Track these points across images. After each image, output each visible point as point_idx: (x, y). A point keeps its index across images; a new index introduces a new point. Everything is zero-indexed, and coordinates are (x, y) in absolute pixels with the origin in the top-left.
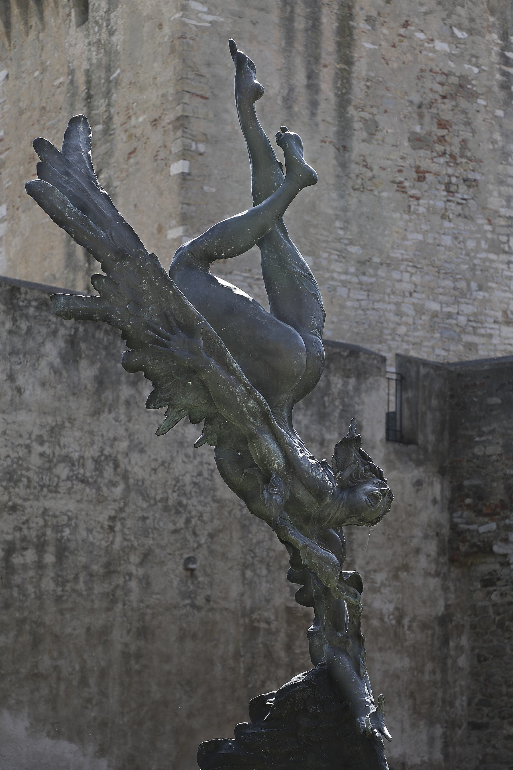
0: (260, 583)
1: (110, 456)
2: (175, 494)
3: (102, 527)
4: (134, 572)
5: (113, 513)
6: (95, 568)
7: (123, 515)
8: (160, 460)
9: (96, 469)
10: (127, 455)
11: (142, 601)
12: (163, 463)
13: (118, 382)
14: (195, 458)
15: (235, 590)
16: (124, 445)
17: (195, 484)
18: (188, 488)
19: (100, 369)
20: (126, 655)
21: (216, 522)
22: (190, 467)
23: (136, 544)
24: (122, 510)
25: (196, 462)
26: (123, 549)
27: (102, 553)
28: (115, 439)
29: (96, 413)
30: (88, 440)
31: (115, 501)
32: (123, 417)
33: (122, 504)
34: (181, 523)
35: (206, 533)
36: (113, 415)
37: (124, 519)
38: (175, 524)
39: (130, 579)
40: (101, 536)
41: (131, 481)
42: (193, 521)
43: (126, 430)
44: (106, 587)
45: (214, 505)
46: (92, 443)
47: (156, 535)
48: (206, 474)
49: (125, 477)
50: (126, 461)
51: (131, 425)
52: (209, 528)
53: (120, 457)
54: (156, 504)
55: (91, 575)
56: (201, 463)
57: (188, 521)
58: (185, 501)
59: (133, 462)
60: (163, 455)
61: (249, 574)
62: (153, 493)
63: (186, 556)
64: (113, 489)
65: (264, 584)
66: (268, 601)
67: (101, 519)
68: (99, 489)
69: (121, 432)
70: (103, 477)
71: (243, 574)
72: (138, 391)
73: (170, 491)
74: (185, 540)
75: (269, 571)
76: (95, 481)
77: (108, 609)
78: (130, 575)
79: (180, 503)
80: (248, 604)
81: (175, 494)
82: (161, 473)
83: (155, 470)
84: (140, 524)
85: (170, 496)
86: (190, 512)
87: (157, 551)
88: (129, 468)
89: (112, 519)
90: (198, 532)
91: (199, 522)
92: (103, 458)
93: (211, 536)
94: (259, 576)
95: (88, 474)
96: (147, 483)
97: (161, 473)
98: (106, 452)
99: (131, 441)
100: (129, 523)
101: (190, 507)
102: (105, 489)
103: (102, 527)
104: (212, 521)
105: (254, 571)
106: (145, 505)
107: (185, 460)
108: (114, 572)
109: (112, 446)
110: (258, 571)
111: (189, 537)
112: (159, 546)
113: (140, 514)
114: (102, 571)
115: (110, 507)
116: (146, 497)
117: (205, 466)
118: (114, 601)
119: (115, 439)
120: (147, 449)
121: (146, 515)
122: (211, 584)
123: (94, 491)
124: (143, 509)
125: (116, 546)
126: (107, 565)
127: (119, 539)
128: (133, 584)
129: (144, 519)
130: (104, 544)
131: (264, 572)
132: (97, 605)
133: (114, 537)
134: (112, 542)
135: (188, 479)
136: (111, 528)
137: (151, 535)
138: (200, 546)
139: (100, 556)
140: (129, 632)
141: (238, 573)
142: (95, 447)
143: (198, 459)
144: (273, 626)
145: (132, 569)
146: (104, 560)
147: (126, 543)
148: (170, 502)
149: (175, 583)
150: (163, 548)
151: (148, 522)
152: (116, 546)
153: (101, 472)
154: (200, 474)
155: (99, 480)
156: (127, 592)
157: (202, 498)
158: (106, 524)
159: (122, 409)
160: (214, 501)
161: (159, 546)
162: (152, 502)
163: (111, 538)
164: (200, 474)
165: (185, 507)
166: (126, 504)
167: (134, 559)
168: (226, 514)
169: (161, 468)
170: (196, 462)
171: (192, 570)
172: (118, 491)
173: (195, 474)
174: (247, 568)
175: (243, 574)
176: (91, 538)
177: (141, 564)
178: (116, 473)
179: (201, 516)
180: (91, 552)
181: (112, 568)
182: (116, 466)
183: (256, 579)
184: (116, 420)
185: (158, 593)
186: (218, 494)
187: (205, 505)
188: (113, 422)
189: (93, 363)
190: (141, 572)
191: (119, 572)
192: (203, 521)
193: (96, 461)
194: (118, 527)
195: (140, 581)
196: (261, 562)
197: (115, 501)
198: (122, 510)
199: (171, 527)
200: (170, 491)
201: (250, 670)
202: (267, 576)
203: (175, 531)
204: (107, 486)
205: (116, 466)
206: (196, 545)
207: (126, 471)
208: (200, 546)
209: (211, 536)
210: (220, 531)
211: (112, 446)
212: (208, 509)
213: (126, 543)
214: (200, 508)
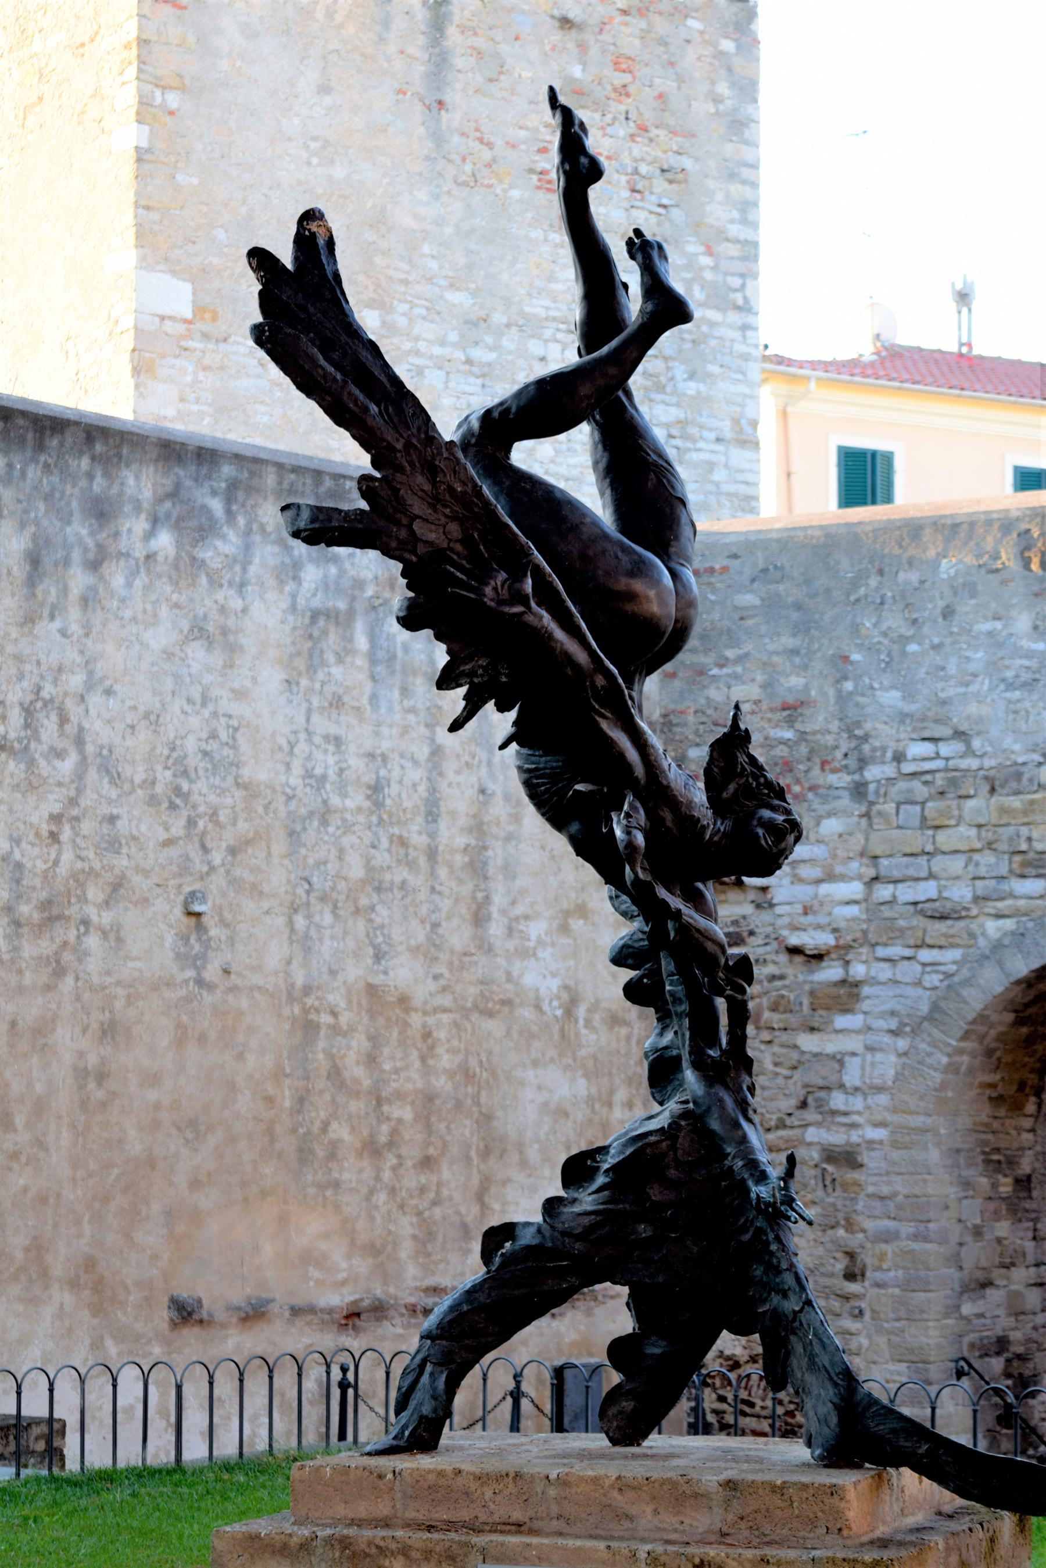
0: (321, 940)
1: (52, 700)
2: (168, 774)
3: (37, 834)
4: (95, 918)
5: (57, 808)
6: (25, 909)
7: (75, 812)
8: (142, 708)
9: (27, 726)
10: (82, 698)
11: (108, 973)
12: (147, 715)
13: (67, 562)
14: (204, 704)
15: (275, 954)
16: (76, 681)
17: (205, 753)
18: (192, 761)
19: (35, 538)
20: (81, 1074)
21: (242, 826)
22: (194, 721)
23: (97, 866)
24: (73, 802)
25: (206, 713)
26: (74, 875)
27: (37, 882)
28: (60, 670)
29: (30, 620)
30: (13, 671)
31: (60, 784)
32: (75, 628)
33: (72, 793)
34: (178, 827)
35: (224, 845)
36: (57, 624)
37: (77, 819)
38: (167, 829)
39: (87, 932)
40: (36, 851)
41: (90, 749)
42: (201, 824)
43: (82, 652)
44: (46, 946)
45: (239, 794)
46: (21, 677)
47: (133, 850)
48: (224, 736)
49: (79, 741)
50: (81, 709)
51: (89, 642)
52: (229, 837)
53: (69, 703)
54: (133, 791)
55: (18, 924)
56: (215, 714)
57: (191, 823)
58: (185, 786)
59: (93, 712)
60: (147, 700)
61: (300, 921)
62: (127, 771)
63: (187, 889)
64: (58, 763)
65: (328, 942)
66: (333, 973)
67: (34, 819)
68: (31, 763)
69: (72, 656)
70: (39, 740)
71: (291, 923)
72: (102, 578)
73: (159, 768)
74: (187, 858)
75: (336, 916)
76: (26, 748)
77: (48, 988)
78: (86, 922)
79: (178, 791)
80: (299, 980)
81: (168, 774)
82: (143, 734)
83: (133, 727)
84: (106, 829)
85: (159, 776)
86: (194, 807)
87: (137, 879)
88: (87, 726)
89: (56, 818)
90: (209, 844)
91: (210, 826)
92: (39, 705)
93: (233, 851)
94: (319, 927)
95: (12, 735)
96: (118, 752)
97: (143, 734)
98: (45, 694)
99: (91, 673)
100: (86, 826)
101: (195, 798)
102: (42, 763)
103: (37, 834)
104: (234, 824)
105: (309, 917)
106: (114, 794)
107: (188, 708)
108: (60, 917)
109: (55, 682)
110: (317, 918)
111: (192, 855)
112: (138, 869)
113: (106, 810)
114: (36, 917)
115: (51, 797)
116: (116, 779)
117: (223, 721)
118: (60, 972)
119: (60, 670)
120: (117, 688)
121: (115, 812)
122: (232, 941)
123: (23, 766)
124: (110, 802)
125: (63, 870)
126: (46, 905)
127: (67, 856)
128: (92, 941)
129: (112, 819)
130: (40, 866)
131: (328, 918)
132: (28, 979)
133: (59, 853)
134: (56, 863)
135: (191, 745)
136: (54, 837)
137: (124, 850)
138: (212, 869)
139: (34, 888)
140: (85, 1030)
141: (281, 921)
142: (25, 684)
143: (211, 707)
144: (344, 1019)
145: (92, 912)
146: (44, 895)
147: (79, 865)
148: (159, 789)
149: (169, 940)
150: (146, 873)
151: (119, 824)
152: (63, 870)
153: (36, 732)
154: (213, 736)
155: (33, 745)
156: (82, 955)
157: (217, 781)
158: (45, 828)
159: (74, 613)
160: (238, 785)
161: (138, 869)
162: (127, 787)
163: (53, 856)
164: (213, 736)
165: (185, 796)
166: (79, 791)
167: (95, 893)
168: (261, 810)
169: (144, 723)
170: (206, 713)
171: (198, 915)
172: (67, 766)
173: (204, 735)
174: (296, 911)
175: (291, 923)
176: (17, 855)
177: (106, 904)
178: (62, 734)
179: (214, 815)
180: (18, 882)
181: (55, 911)
182: (63, 720)
183: (313, 932)
184: (63, 633)
185: (136, 959)
186: (246, 772)
187: (223, 792)
188: (58, 637)
189: (23, 525)
190: (106, 918)
191: (68, 919)
192: (217, 823)
193: (28, 711)
194: (66, 834)
195: (105, 935)
196: (323, 899)
197: (60, 784)
198: (73, 802)
199: (163, 835)
200: (159, 768)
201: (301, 1101)
202: (332, 927)
203: (168, 843)
204: (46, 757)
205: (63, 720)
206: (205, 869)
207: (81, 729)
208: (212, 869)
209: (233, 851)
210: (248, 842)
211: (55, 682)
212: (229, 801)
213: (79, 865)
214: (212, 798)
